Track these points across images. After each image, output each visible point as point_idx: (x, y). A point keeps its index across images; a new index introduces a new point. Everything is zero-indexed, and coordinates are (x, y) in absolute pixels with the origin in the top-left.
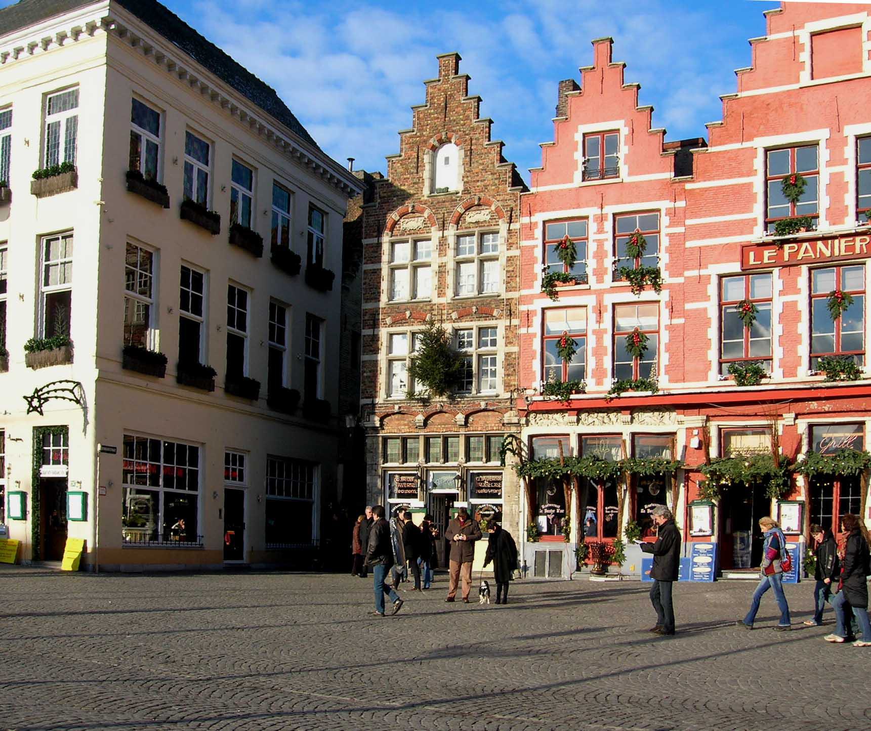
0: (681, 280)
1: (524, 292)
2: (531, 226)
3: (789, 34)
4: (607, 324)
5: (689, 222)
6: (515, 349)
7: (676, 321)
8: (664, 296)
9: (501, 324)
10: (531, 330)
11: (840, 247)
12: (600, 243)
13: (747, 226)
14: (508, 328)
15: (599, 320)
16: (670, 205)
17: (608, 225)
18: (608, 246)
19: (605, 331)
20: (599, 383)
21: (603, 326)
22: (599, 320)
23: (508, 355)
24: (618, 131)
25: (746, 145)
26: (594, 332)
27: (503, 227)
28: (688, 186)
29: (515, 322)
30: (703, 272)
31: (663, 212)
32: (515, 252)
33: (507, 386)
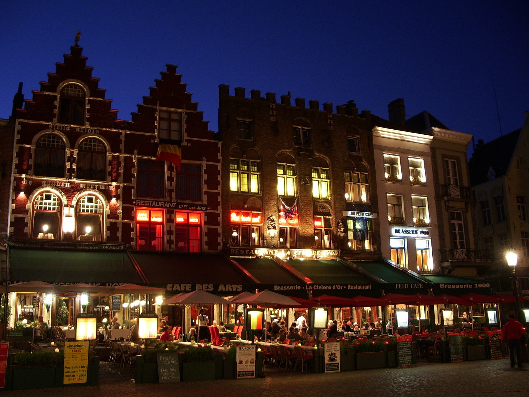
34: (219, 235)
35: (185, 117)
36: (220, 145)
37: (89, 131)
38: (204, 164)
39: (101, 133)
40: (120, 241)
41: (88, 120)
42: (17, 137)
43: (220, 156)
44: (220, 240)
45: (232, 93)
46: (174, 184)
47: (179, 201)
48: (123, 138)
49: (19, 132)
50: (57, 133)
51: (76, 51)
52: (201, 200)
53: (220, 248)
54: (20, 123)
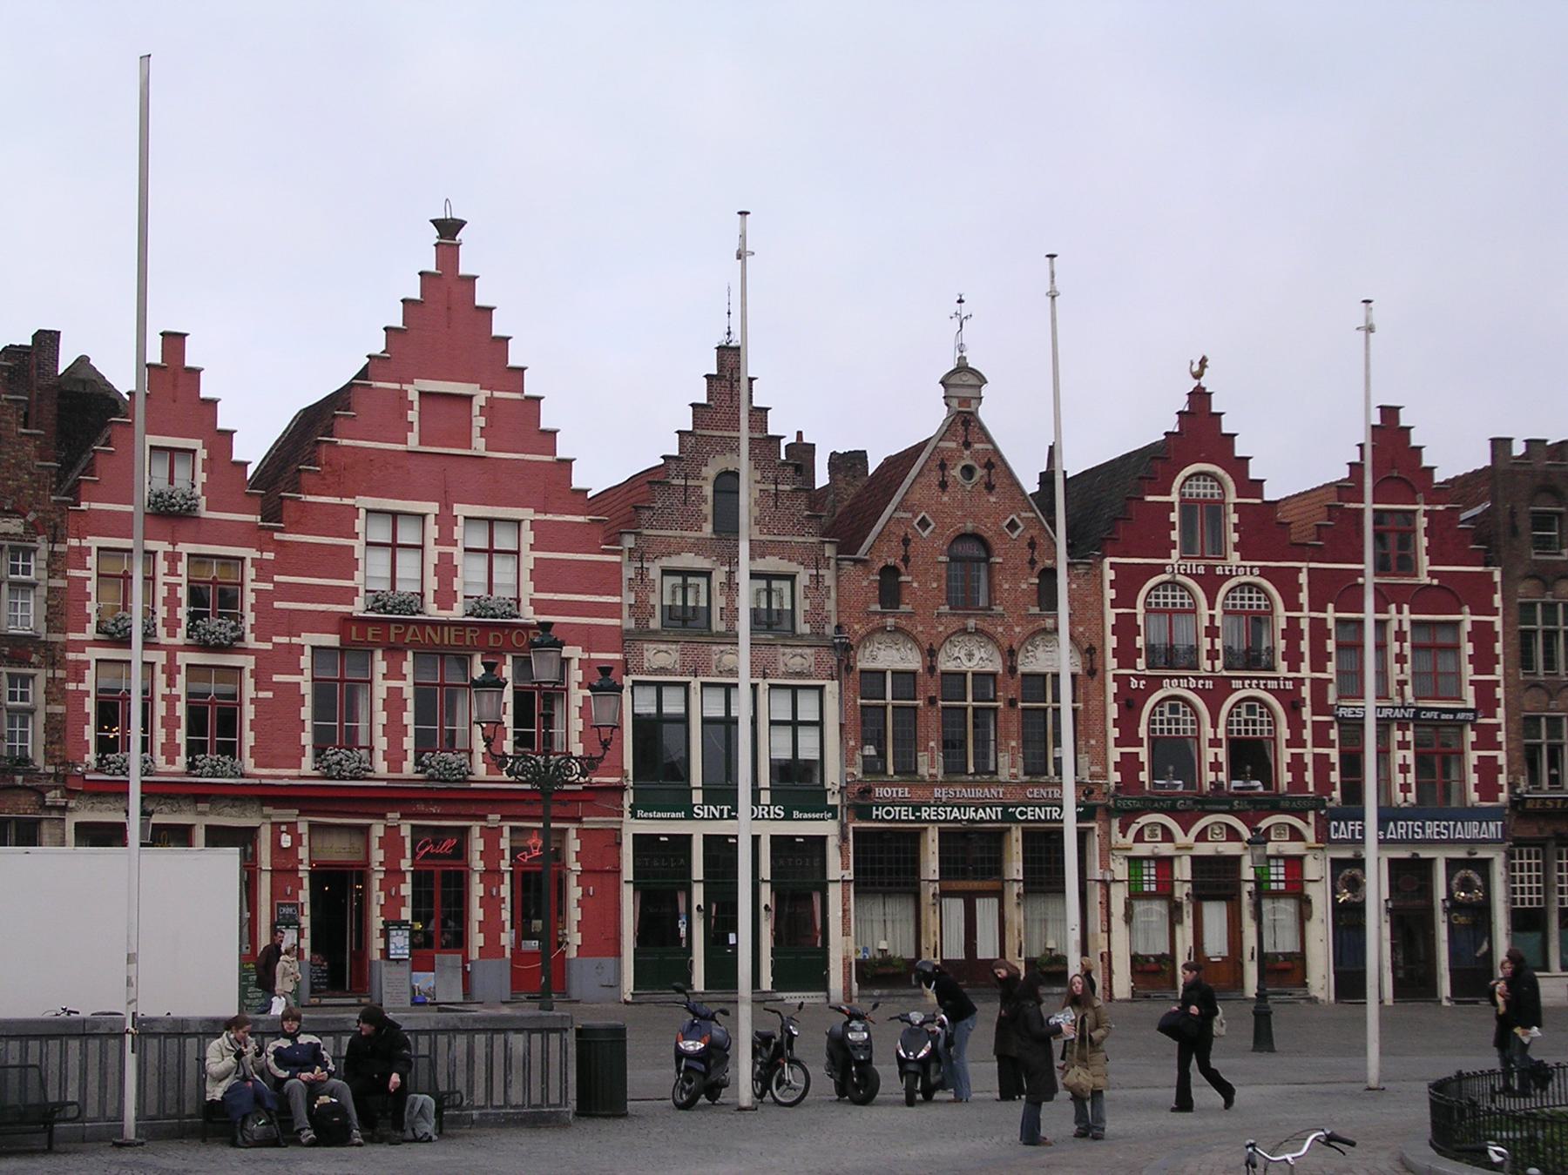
0: (269, 646)
1: (72, 636)
2: (83, 552)
3: (396, 386)
4: (181, 688)
5: (276, 578)
6: (59, 709)
7: (262, 695)
8: (248, 663)
9: (42, 675)
10: (82, 687)
11: (449, 637)
12: (172, 588)
13: (349, 595)
14: (51, 681)
15: (171, 683)
16: (257, 555)
17: (182, 567)
18: (183, 593)
19: (178, 698)
20: (170, 761)
21: (174, 691)
22: (171, 683)
23: (49, 716)
24: (194, 451)
25: (346, 501)
26: (164, 697)
27: (43, 545)
28: (277, 536)
29: (60, 674)
30: (295, 640)
31: (248, 562)
32: (58, 583)
33: (49, 757)
34: (1499, 770)
35: (1422, 522)
36: (1497, 577)
37: (1241, 571)
38: (1467, 619)
39: (1264, 572)
40: (1311, 789)
41: (1237, 547)
42: (1110, 594)
43: (1497, 600)
44: (1502, 779)
45: (1518, 449)
46: (1407, 667)
47: (1420, 704)
48: (1303, 578)
49: (1113, 584)
50: (1179, 578)
51: (1200, 397)
52: (1460, 699)
53: (1503, 797)
54: (1112, 566)
